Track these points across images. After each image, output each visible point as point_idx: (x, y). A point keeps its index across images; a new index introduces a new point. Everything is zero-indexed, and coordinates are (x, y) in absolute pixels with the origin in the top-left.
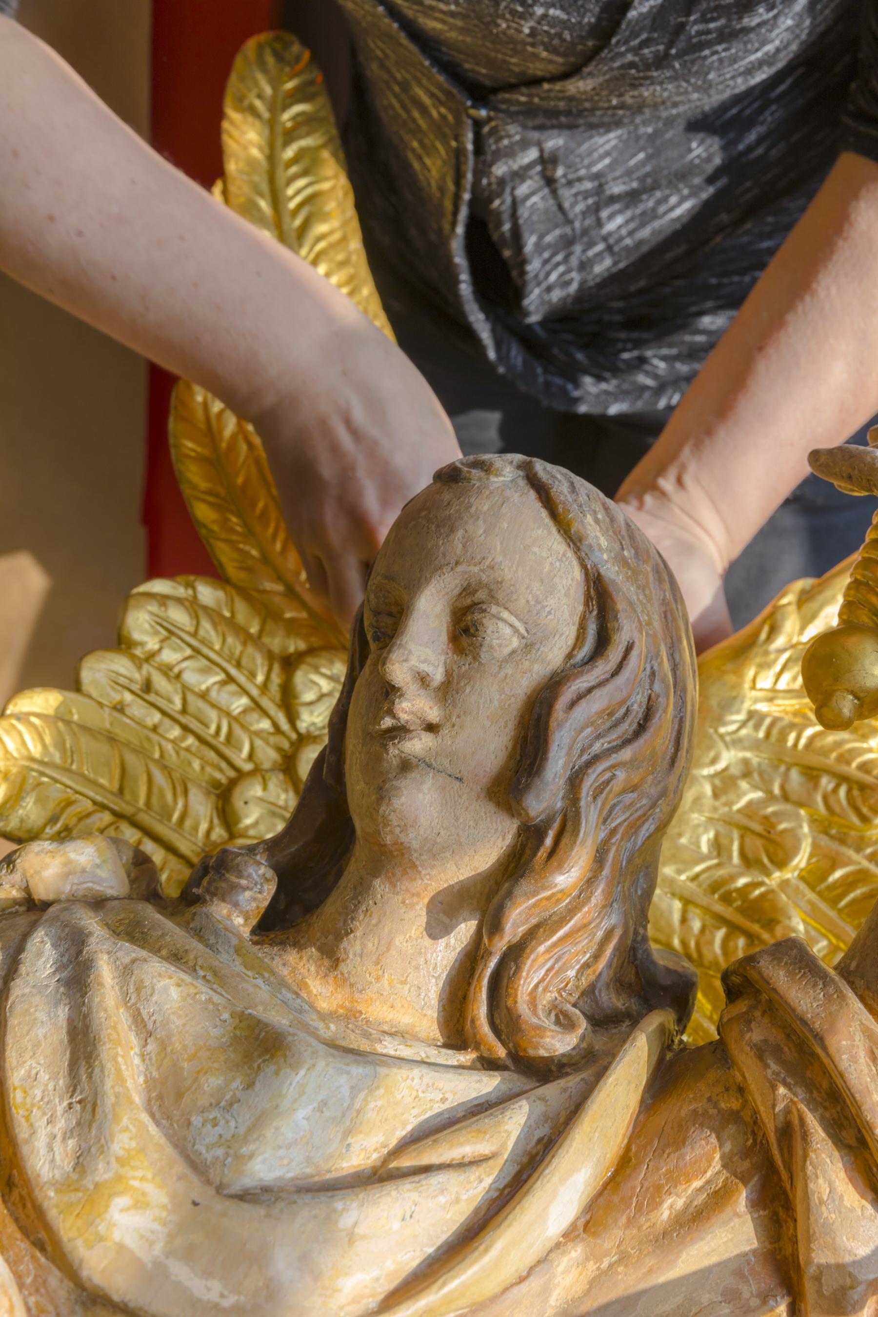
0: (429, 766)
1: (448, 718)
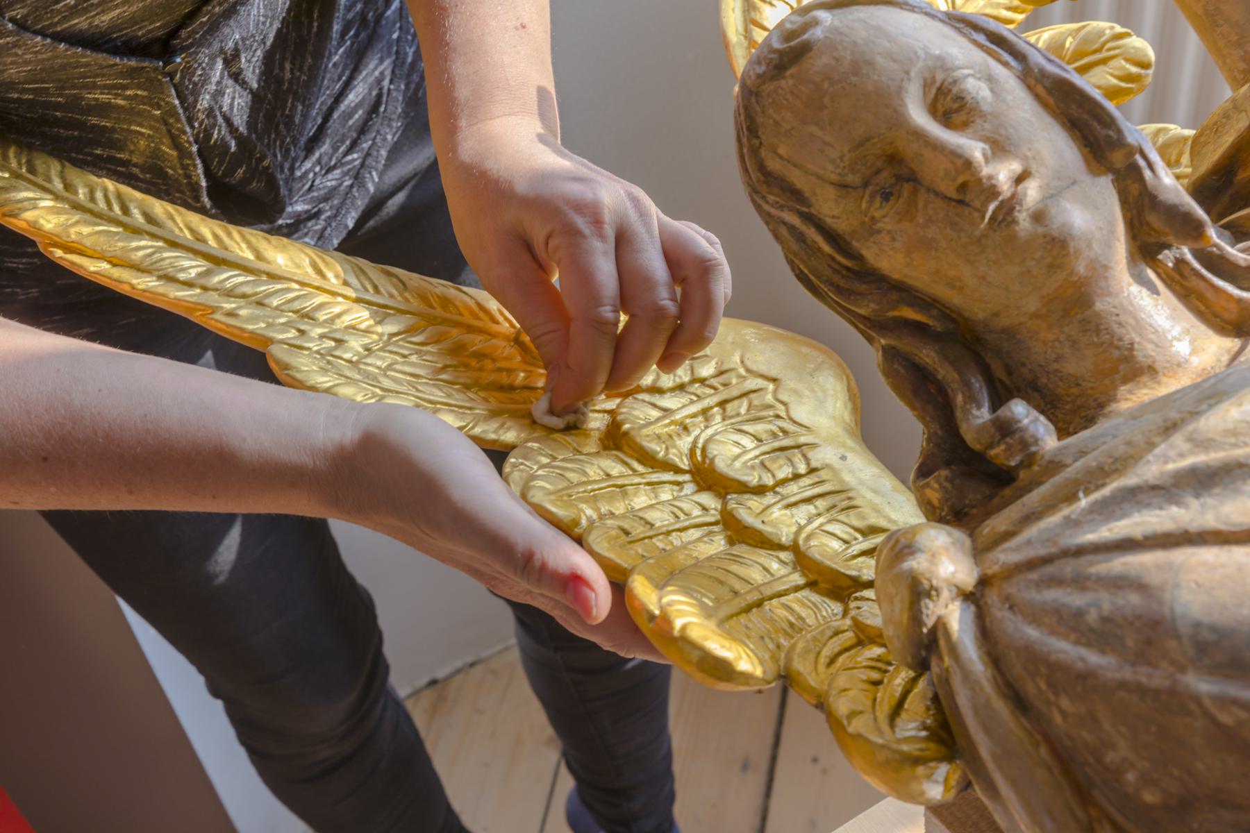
0: (1052, 196)
1: (1025, 159)
